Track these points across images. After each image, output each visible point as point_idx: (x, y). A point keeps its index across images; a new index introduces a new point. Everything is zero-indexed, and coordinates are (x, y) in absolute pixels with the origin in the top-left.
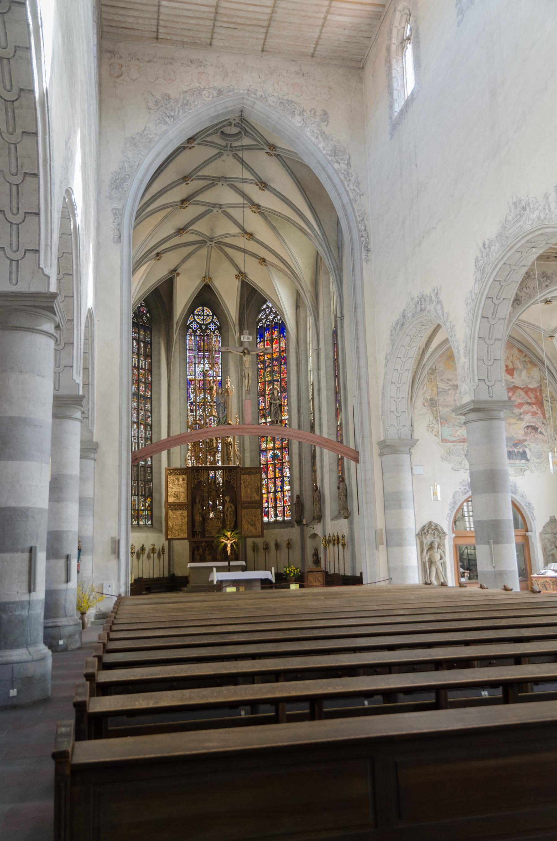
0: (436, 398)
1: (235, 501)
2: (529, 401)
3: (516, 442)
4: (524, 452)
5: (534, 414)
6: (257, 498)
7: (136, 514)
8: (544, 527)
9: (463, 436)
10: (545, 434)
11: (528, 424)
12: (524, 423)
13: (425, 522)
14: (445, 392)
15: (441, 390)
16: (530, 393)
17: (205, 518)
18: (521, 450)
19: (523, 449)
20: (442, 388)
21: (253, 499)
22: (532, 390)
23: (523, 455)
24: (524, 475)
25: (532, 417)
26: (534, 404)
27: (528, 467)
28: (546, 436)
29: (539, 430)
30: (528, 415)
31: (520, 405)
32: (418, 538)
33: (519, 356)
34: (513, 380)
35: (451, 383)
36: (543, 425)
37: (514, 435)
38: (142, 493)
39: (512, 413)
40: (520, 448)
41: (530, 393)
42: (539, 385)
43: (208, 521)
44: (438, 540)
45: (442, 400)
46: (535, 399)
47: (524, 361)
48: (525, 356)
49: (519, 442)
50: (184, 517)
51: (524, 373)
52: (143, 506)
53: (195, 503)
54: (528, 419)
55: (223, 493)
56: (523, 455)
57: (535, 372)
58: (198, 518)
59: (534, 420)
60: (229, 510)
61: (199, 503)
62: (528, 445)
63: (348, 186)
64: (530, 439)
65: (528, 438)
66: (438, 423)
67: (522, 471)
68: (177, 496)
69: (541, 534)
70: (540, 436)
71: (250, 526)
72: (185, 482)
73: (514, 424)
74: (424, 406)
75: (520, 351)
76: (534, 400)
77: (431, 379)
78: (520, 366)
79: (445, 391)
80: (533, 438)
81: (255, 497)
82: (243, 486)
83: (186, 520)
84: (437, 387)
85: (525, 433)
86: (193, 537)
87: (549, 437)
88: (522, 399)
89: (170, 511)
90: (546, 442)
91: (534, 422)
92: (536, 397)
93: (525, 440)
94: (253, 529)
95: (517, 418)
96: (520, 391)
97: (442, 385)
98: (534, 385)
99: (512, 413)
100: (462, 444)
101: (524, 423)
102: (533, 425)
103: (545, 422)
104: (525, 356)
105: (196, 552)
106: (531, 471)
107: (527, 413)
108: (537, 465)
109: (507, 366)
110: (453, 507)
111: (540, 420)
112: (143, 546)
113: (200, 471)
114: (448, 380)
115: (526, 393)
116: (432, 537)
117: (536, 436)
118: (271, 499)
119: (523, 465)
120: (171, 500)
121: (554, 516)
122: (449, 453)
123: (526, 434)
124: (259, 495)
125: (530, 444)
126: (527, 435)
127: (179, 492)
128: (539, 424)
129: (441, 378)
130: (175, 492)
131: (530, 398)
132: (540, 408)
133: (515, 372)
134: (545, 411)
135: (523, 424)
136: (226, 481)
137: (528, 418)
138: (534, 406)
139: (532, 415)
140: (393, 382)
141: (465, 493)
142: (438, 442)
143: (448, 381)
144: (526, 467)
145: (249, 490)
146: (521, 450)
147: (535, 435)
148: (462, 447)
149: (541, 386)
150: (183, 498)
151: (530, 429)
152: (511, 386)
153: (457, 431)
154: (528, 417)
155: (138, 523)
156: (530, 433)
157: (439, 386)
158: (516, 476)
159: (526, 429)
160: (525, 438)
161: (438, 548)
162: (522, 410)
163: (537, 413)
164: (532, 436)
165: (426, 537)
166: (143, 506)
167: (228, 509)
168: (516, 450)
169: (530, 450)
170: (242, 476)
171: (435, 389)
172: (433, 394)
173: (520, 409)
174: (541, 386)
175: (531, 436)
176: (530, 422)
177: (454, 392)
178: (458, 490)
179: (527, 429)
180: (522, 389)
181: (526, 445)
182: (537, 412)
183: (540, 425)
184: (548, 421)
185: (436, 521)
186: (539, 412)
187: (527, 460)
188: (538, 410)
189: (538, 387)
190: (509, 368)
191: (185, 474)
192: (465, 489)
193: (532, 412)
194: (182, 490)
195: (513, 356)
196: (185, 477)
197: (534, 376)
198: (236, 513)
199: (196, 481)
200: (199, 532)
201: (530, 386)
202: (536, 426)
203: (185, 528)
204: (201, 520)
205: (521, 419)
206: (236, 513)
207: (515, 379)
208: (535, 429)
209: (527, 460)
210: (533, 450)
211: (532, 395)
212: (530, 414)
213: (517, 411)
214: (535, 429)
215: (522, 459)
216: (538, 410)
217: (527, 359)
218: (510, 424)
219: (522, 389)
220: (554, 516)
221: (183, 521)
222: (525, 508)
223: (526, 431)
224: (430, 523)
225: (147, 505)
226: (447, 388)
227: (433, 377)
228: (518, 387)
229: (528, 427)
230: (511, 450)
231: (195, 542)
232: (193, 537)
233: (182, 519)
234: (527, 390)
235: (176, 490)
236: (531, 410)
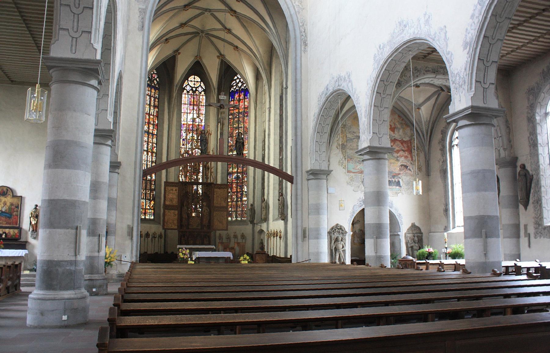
0: (345, 144)
2: (403, 149)
4: (399, 181)
5: (406, 157)
6: (225, 205)
7: (144, 212)
8: (408, 229)
9: (361, 169)
10: (412, 170)
13: (334, 224)
14: (351, 140)
15: (349, 139)
16: (404, 144)
17: (189, 216)
18: (397, 180)
20: (349, 138)
21: (222, 205)
22: (405, 142)
23: (398, 184)
25: (405, 159)
26: (406, 151)
27: (400, 191)
28: (413, 172)
29: (408, 168)
31: (398, 151)
32: (329, 234)
33: (398, 120)
34: (394, 135)
35: (355, 135)
39: (393, 156)
41: (404, 144)
43: (191, 218)
44: (341, 236)
45: (349, 145)
47: (401, 123)
48: (403, 120)
51: (401, 131)
54: (402, 160)
55: (202, 200)
56: (398, 184)
57: (408, 131)
58: (185, 216)
59: (406, 161)
60: (206, 211)
62: (402, 177)
63: (295, 3)
65: (401, 172)
66: (345, 160)
67: (397, 193)
68: (171, 200)
69: (405, 234)
70: (409, 171)
72: (177, 192)
73: (393, 163)
74: (338, 148)
75: (399, 116)
76: (406, 148)
77: (343, 131)
78: (399, 126)
79: (351, 140)
80: (405, 172)
82: (215, 196)
83: (177, 217)
84: (346, 137)
85: (400, 169)
87: (415, 172)
88: (399, 147)
89: (166, 210)
90: (412, 176)
91: (405, 163)
92: (408, 147)
93: (399, 174)
95: (395, 159)
96: (398, 142)
97: (349, 136)
98: (406, 139)
99: (393, 156)
100: (360, 174)
102: (405, 164)
104: (403, 120)
105: (183, 239)
107: (402, 157)
108: (406, 190)
109: (391, 126)
110: (353, 215)
112: (148, 232)
114: (354, 132)
115: (402, 144)
116: (338, 234)
117: (407, 171)
118: (234, 206)
119: (398, 190)
120: (168, 203)
121: (414, 223)
122: (352, 180)
123: (400, 170)
125: (403, 176)
127: (173, 198)
128: (408, 164)
129: (349, 131)
132: (410, 154)
133: (395, 130)
135: (399, 164)
136: (204, 192)
138: (406, 152)
139: (405, 158)
140: (318, 131)
141: (361, 206)
142: (345, 173)
143: (354, 133)
144: (399, 191)
145: (219, 199)
146: (397, 180)
148: (360, 177)
149: (411, 140)
150: (175, 202)
151: (403, 167)
152: (393, 139)
153: (357, 167)
154: (402, 159)
155: (145, 217)
157: (347, 136)
158: (393, 196)
160: (400, 172)
161: (342, 240)
162: (399, 155)
164: (404, 171)
165: (334, 234)
167: (205, 211)
168: (393, 180)
169: (402, 180)
170: (215, 189)
171: (345, 137)
172: (344, 141)
173: (398, 153)
174: (411, 140)
176: (403, 162)
177: (357, 140)
178: (356, 204)
180: (400, 141)
181: (400, 177)
184: (414, 162)
185: (341, 224)
186: (409, 156)
187: (400, 187)
189: (409, 140)
190: (392, 127)
192: (360, 204)
193: (405, 156)
194: (175, 197)
195: (395, 119)
196: (177, 188)
198: (210, 213)
203: (176, 222)
205: (398, 160)
206: (210, 213)
207: (396, 134)
208: (406, 167)
209: (400, 187)
210: (404, 180)
211: (405, 145)
212: (404, 157)
213: (395, 155)
214: (406, 167)
215: (397, 186)
217: (403, 122)
218: (391, 163)
219: (400, 141)
220: (414, 223)
222: (397, 217)
224: (337, 224)
225: (151, 206)
226: (352, 137)
227: (344, 130)
228: (397, 140)
229: (402, 165)
230: (390, 179)
234: (402, 142)
235: (171, 197)
236: (404, 155)
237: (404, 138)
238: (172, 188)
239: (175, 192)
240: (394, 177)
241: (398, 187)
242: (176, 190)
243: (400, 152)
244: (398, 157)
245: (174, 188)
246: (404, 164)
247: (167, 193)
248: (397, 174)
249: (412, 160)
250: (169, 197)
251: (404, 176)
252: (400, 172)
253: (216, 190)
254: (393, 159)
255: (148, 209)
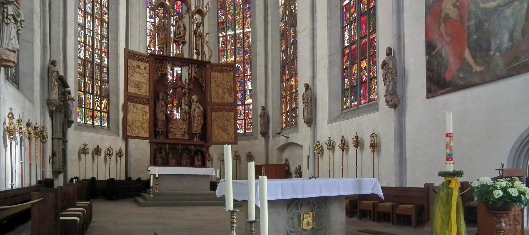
1: (203, 101)
6: (230, 100)
7: (90, 114)
17: (169, 118)
21: (225, 101)
38: (97, 92)
43: (172, 122)
50: (146, 113)
52: (98, 106)
53: (158, 99)
58: (161, 117)
60: (197, 110)
61: (162, 99)
71: (221, 131)
72: (148, 72)
81: (227, 99)
82: (213, 85)
83: (148, 117)
86: (155, 137)
89: (129, 103)
94: (224, 135)
105: (158, 155)
113: (165, 62)
124: (232, 97)
127: (140, 83)
130: (136, 81)
145: (220, 90)
150: (145, 91)
166: (98, 106)
167: (195, 109)
170: (212, 73)
191: (148, 62)
196: (147, 65)
199: (160, 73)
200: (162, 132)
203: (146, 125)
204: (165, 119)
221: (144, 117)
225: (103, 106)
231: (157, 144)
232: (155, 137)
233: (143, 115)
235: (137, 79)
238: (139, 63)
239: (145, 71)
242: (145, 68)
245: (143, 65)
247: (130, 72)
250: (134, 78)
253: (214, 74)
255: (98, 111)
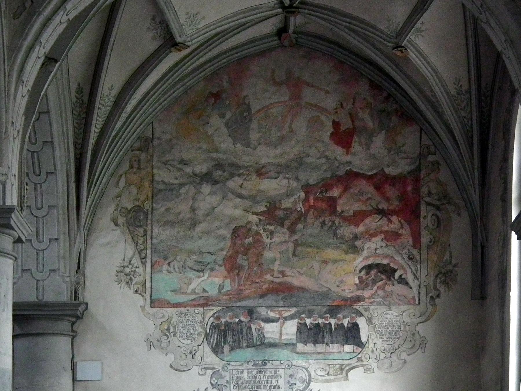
2: (384, 205)
3: (335, 303)
4: (355, 327)
10: (414, 283)
11: (371, 261)
12: (361, 259)
18: (346, 322)
19: (352, 318)
22: (393, 180)
24: (347, 378)
25: (383, 244)
26: (394, 212)
27: (359, 360)
28: (415, 289)
29: (397, 275)
30: (374, 239)
36: (410, 262)
37: (334, 289)
40: (344, 317)
42: (413, 167)
46: (400, 201)
49: (343, 303)
59: (389, 251)
62: (367, 310)
64: (372, 296)
65: (366, 293)
73: (335, 262)
76: (396, 204)
80: (380, 292)
88: (365, 202)
90: (411, 302)
91: (386, 256)
92: (403, 197)
93: (359, 299)
95: (344, 247)
101: (361, 259)
102: (385, 262)
103: (417, 256)
106: (367, 370)
107: (372, 236)
108: (382, 355)
111: (406, 251)
115: (378, 188)
117: (388, 288)
119: (348, 356)
123: (363, 284)
125: (372, 307)
126: (367, 285)
131: (388, 199)
132: (409, 223)
134: (422, 228)
135: (360, 261)
137: (373, 246)
138: (394, 218)
146: (346, 322)
147: (387, 288)
149: (419, 169)
151: (373, 272)
156: (374, 282)
159: (364, 272)
160: (359, 293)
162: (361, 228)
163: (401, 235)
169: (370, 321)
173: (357, 225)
174: (419, 169)
175: (375, 288)
176: (376, 255)
179: (367, 274)
181: (361, 310)
182: (401, 231)
183: (403, 262)
186: (406, 231)
187: (360, 344)
188: (402, 227)
189: (409, 173)
193: (386, 233)
197: (403, 146)
201: (391, 171)
202: (392, 265)
205: (354, 250)
210: (375, 321)
211: (391, 192)
215: (347, 342)
216: (402, 227)
223: (364, 277)
229: (369, 268)
236: (386, 228)
237: (388, 166)
240: (337, 313)
241: (348, 348)
243: (367, 221)
244: (356, 237)
246: (378, 261)
248: (346, 300)
249: (417, 243)
251: (379, 304)
252: (359, 293)
254: (337, 248)
